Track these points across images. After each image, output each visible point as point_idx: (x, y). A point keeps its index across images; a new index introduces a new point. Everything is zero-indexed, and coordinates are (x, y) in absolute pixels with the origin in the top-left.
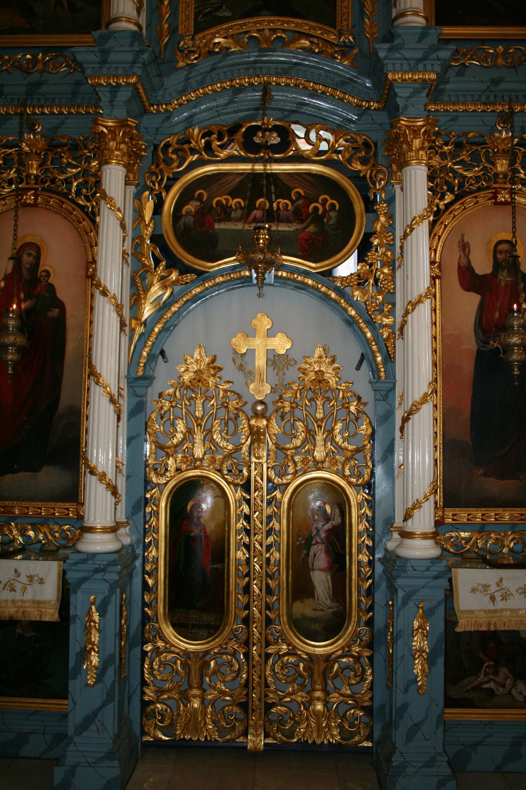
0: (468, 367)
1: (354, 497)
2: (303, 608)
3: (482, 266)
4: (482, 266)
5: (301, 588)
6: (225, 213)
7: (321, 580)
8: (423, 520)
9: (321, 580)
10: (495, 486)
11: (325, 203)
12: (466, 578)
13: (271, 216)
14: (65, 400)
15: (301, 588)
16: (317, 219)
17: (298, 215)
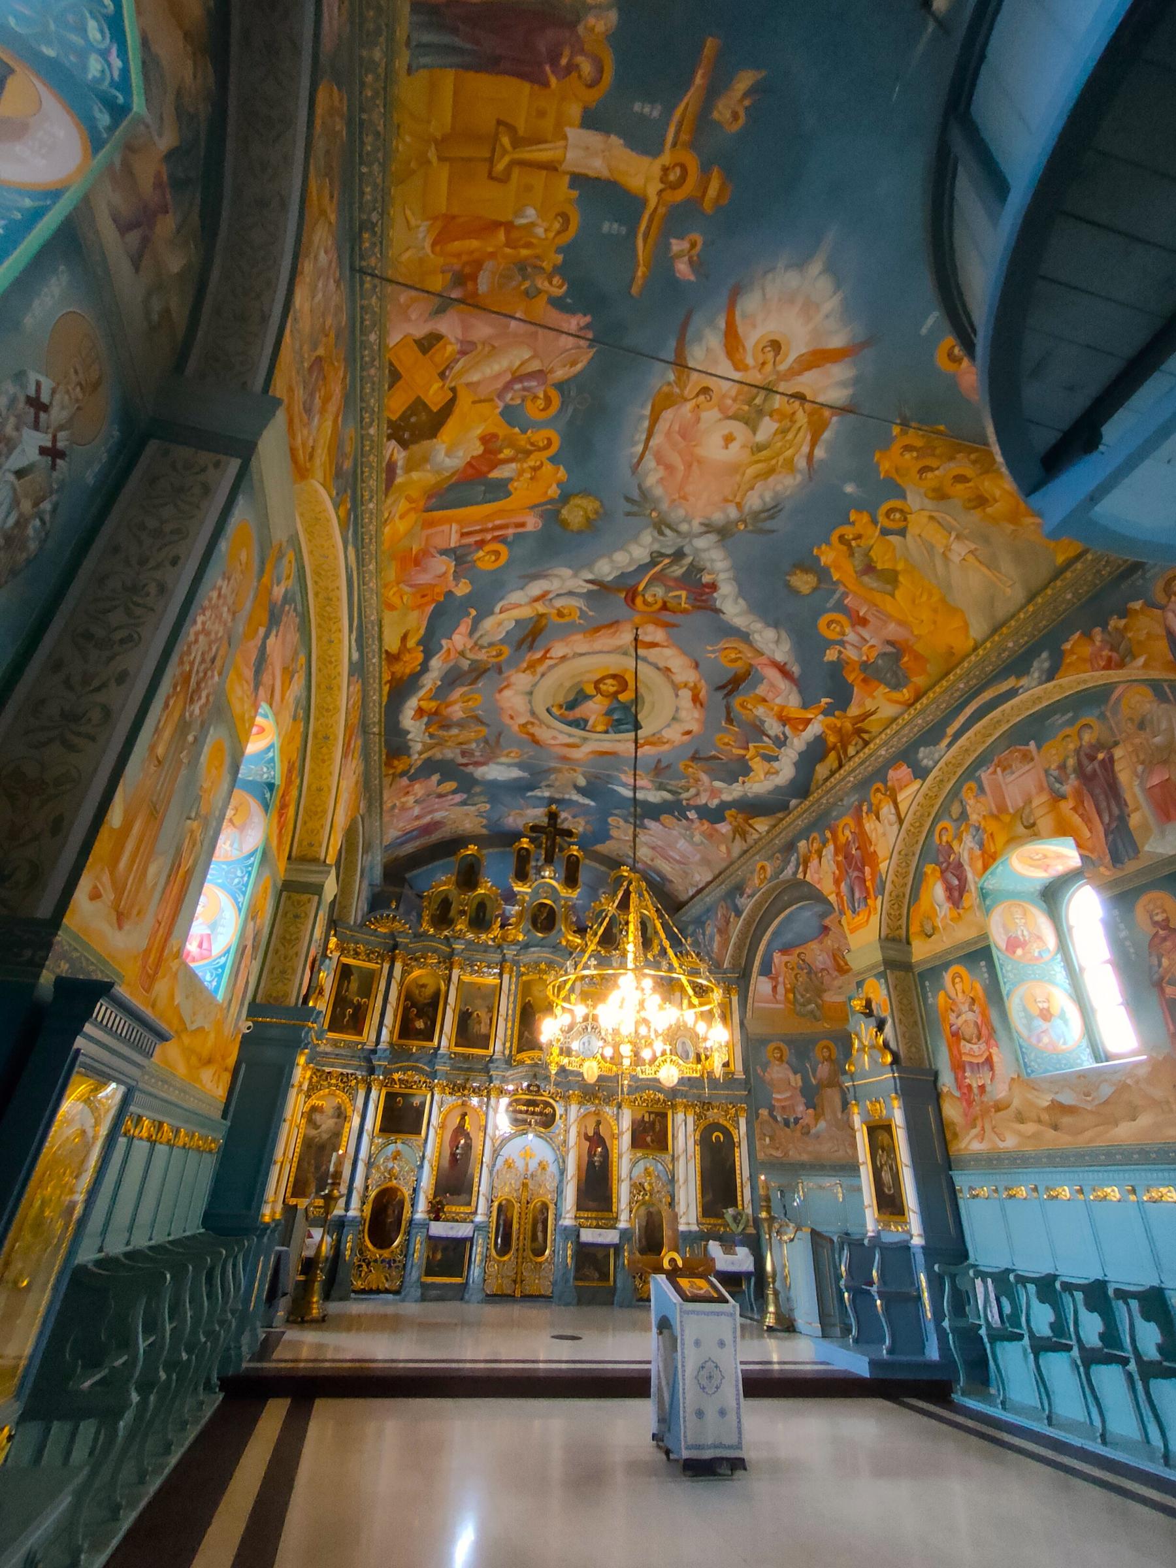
0: (584, 1166)
1: (552, 1207)
2: (536, 1245)
3: (591, 1134)
4: (591, 1134)
5: (534, 1238)
6: (521, 1112)
7: (540, 1235)
8: (572, 1214)
9: (540, 1235)
10: (591, 1204)
11: (548, 1110)
12: (582, 1230)
13: (533, 1113)
14: (470, 1171)
15: (534, 1238)
16: (546, 1115)
17: (541, 1114)
